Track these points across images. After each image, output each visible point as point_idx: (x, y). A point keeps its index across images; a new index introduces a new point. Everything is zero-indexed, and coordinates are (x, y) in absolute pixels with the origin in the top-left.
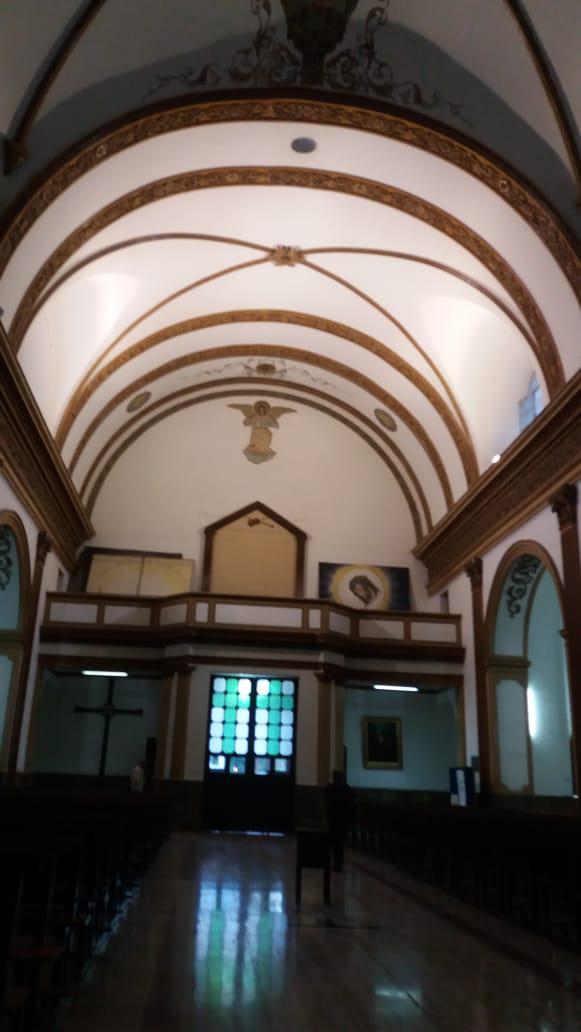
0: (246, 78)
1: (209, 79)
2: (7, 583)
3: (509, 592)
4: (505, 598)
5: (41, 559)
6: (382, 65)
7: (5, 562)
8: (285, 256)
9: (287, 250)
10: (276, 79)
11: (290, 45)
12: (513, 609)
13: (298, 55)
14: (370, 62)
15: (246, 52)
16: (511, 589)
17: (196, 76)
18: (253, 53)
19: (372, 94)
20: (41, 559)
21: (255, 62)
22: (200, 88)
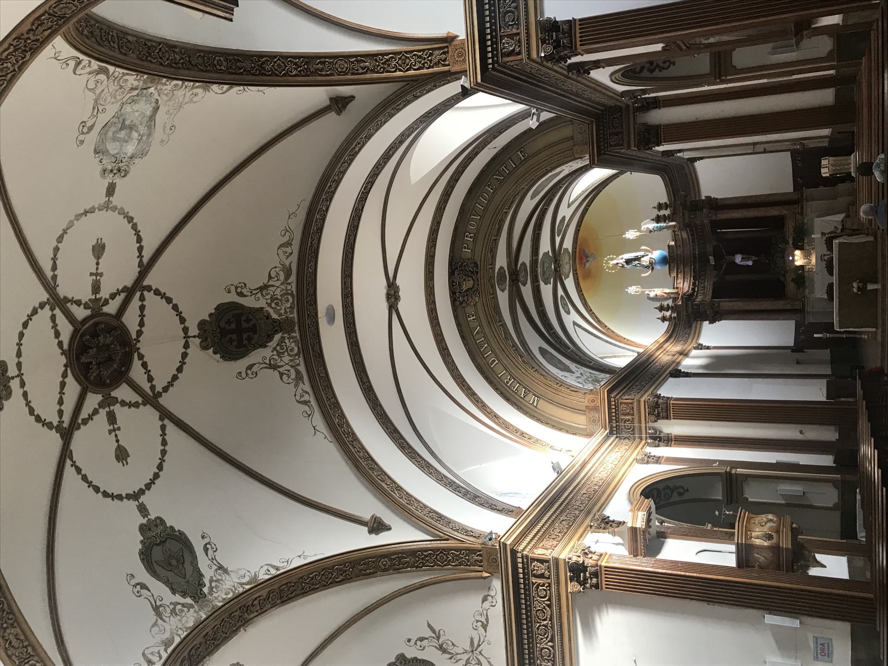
0: (298, 373)
1: (306, 397)
2: (683, 488)
3: (652, 71)
4: (657, 73)
5: (658, 460)
6: (270, 277)
7: (668, 491)
8: (393, 295)
9: (388, 296)
10: (296, 351)
11: (273, 344)
12: (668, 64)
13: (277, 337)
14: (273, 286)
15: (281, 375)
16: (649, 70)
17: (306, 408)
18: (281, 370)
19: (293, 278)
20: (658, 460)
21: (287, 367)
22: (313, 403)
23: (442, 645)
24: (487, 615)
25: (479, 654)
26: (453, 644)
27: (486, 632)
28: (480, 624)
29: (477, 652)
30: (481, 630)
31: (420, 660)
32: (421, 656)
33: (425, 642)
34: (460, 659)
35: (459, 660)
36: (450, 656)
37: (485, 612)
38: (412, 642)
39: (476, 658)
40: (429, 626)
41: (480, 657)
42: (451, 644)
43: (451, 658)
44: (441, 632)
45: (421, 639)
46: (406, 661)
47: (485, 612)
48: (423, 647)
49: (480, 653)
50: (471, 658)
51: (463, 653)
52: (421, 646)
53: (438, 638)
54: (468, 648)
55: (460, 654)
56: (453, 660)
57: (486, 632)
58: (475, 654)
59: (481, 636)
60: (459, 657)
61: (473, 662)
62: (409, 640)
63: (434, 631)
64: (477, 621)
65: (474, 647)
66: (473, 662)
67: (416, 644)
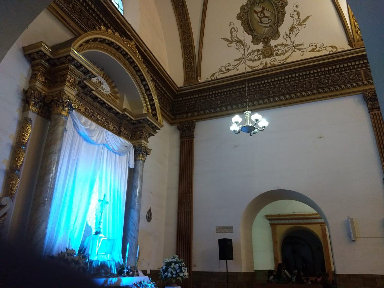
23: (295, 28)
24: (322, 50)
25: (293, 50)
26: (296, 34)
27: (309, 52)
28: (314, 47)
29: (294, 49)
30: (310, 49)
31: (284, 16)
32: (287, 16)
33: (296, 17)
34: (287, 41)
35: (286, 40)
36: (288, 34)
37: (324, 49)
38: (295, 9)
39: (290, 49)
40: (308, 18)
41: (290, 51)
42: (296, 33)
43: (286, 35)
44: (304, 26)
45: (298, 14)
46: (283, 6)
47: (324, 49)
48: (293, 16)
49: (293, 51)
50: (288, 47)
51: (292, 42)
52: (293, 15)
53: (300, 25)
54: (295, 43)
55: (290, 40)
56: (285, 36)
57: (309, 52)
58: (292, 48)
59: (306, 49)
60: (288, 39)
61: (286, 48)
62: (297, 6)
63: (304, 21)
64: (316, 46)
65: (296, 47)
66: (286, 48)
67: (295, 11)
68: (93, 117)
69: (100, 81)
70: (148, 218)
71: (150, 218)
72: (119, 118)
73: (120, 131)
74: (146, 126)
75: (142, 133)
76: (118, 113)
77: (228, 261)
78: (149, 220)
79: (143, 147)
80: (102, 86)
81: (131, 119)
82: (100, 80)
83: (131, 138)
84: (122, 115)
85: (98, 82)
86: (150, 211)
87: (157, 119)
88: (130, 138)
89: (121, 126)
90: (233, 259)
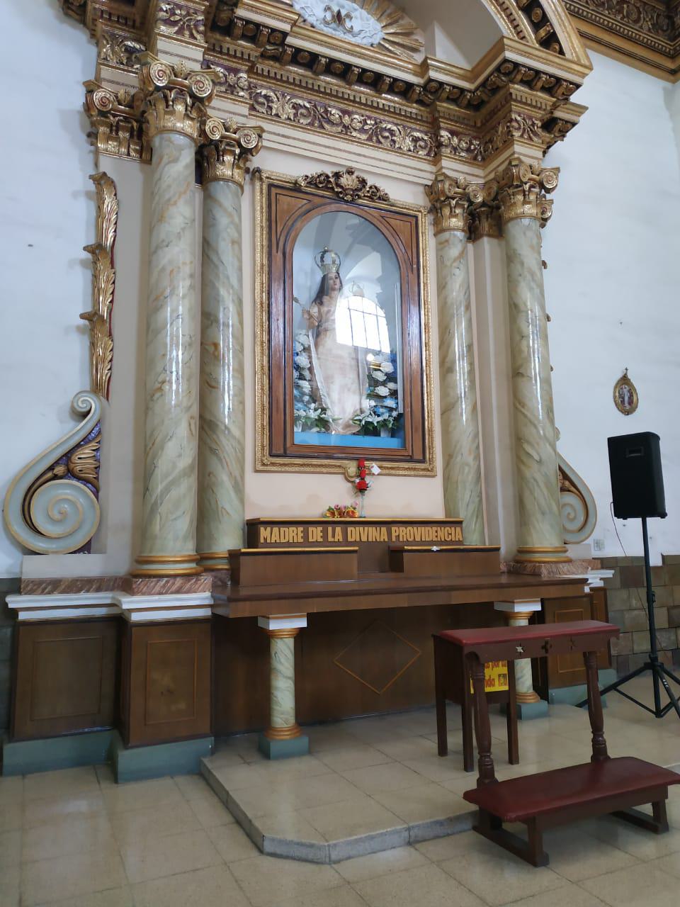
68: (326, 126)
69: (339, 12)
70: (623, 402)
71: (631, 402)
72: (420, 102)
73: (440, 145)
74: (517, 89)
75: (511, 120)
76: (409, 86)
77: (649, 520)
78: (628, 407)
79: (515, 166)
80: (348, 24)
81: (462, 90)
82: (336, 9)
83: (483, 159)
84: (425, 87)
85: (333, 16)
86: (625, 380)
87: (561, 52)
88: (479, 158)
89: (440, 128)
90: (663, 515)
